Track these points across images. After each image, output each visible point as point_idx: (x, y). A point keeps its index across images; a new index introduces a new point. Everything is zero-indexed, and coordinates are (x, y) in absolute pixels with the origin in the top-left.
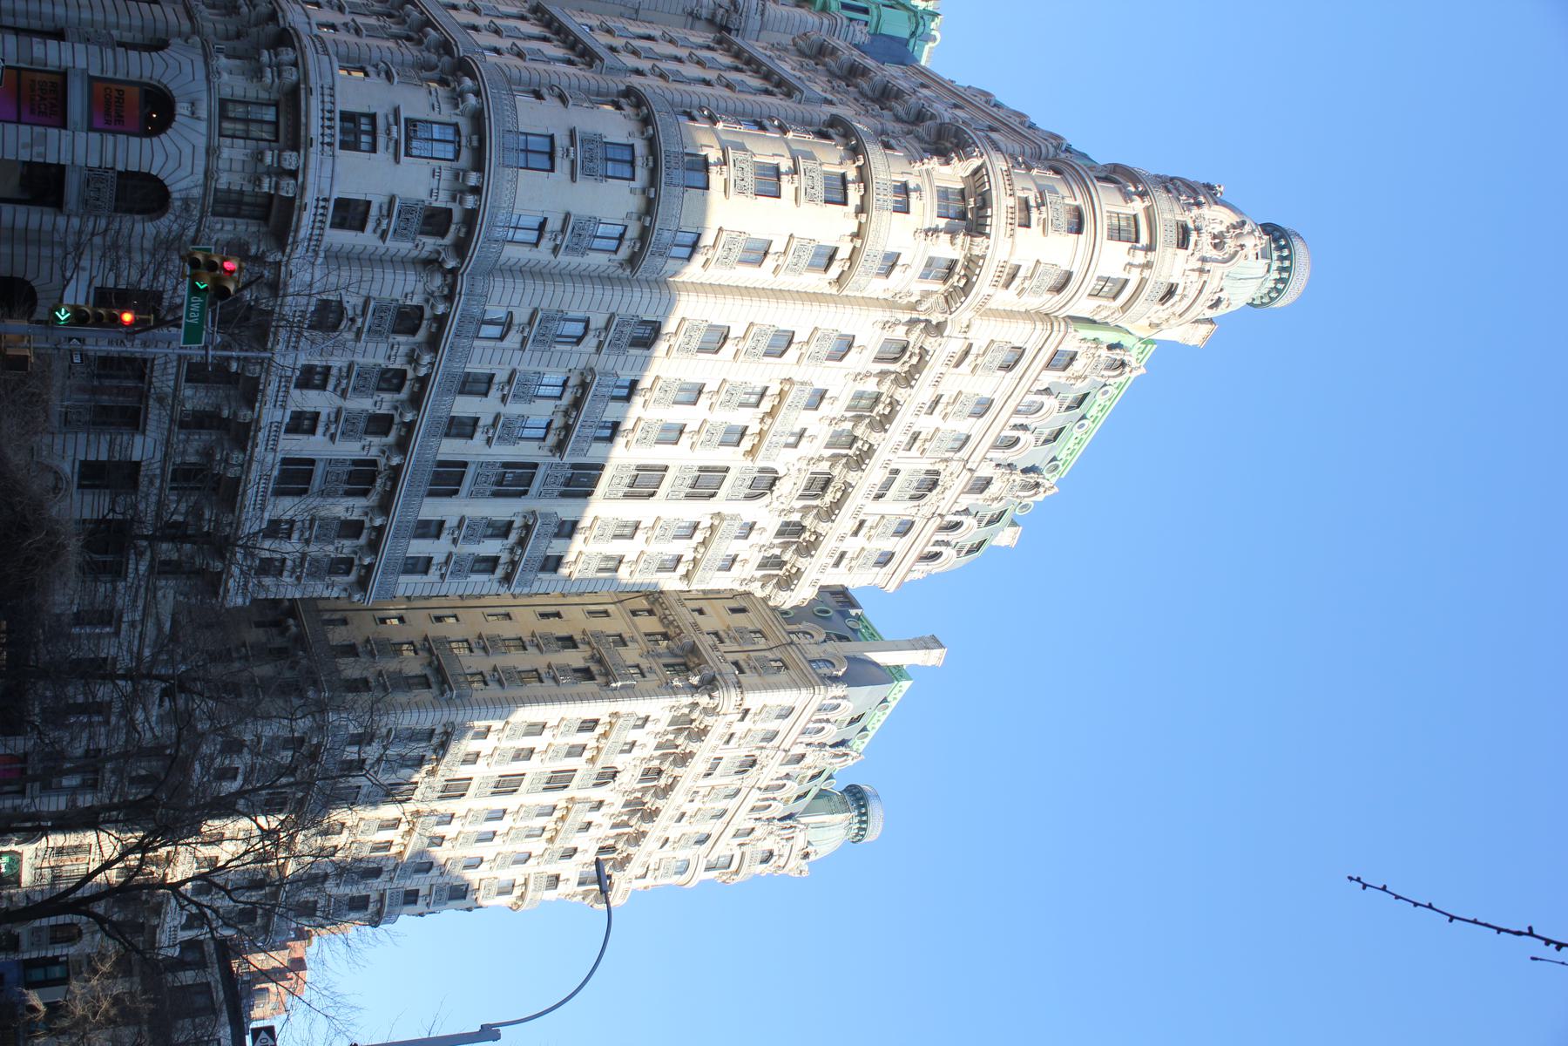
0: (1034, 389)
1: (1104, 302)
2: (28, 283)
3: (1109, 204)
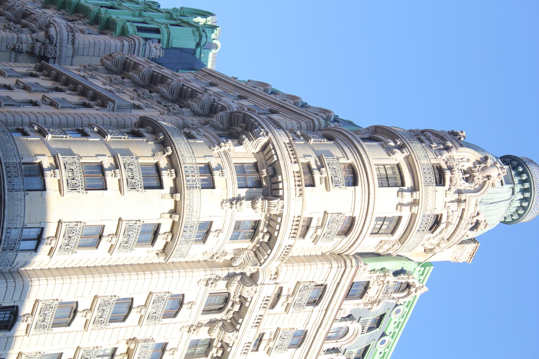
0: (339, 317)
1: (384, 238)
3: (376, 158)
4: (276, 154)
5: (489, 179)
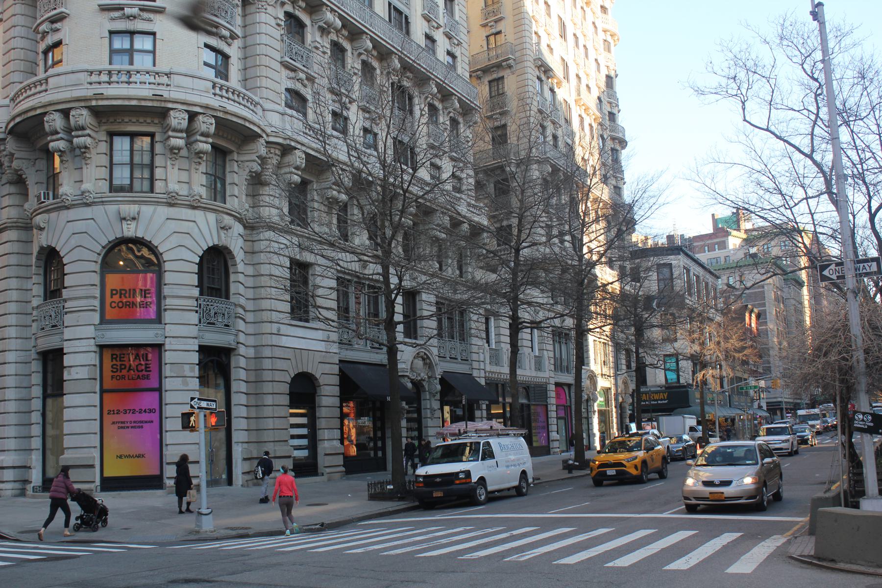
2: (292, 379)
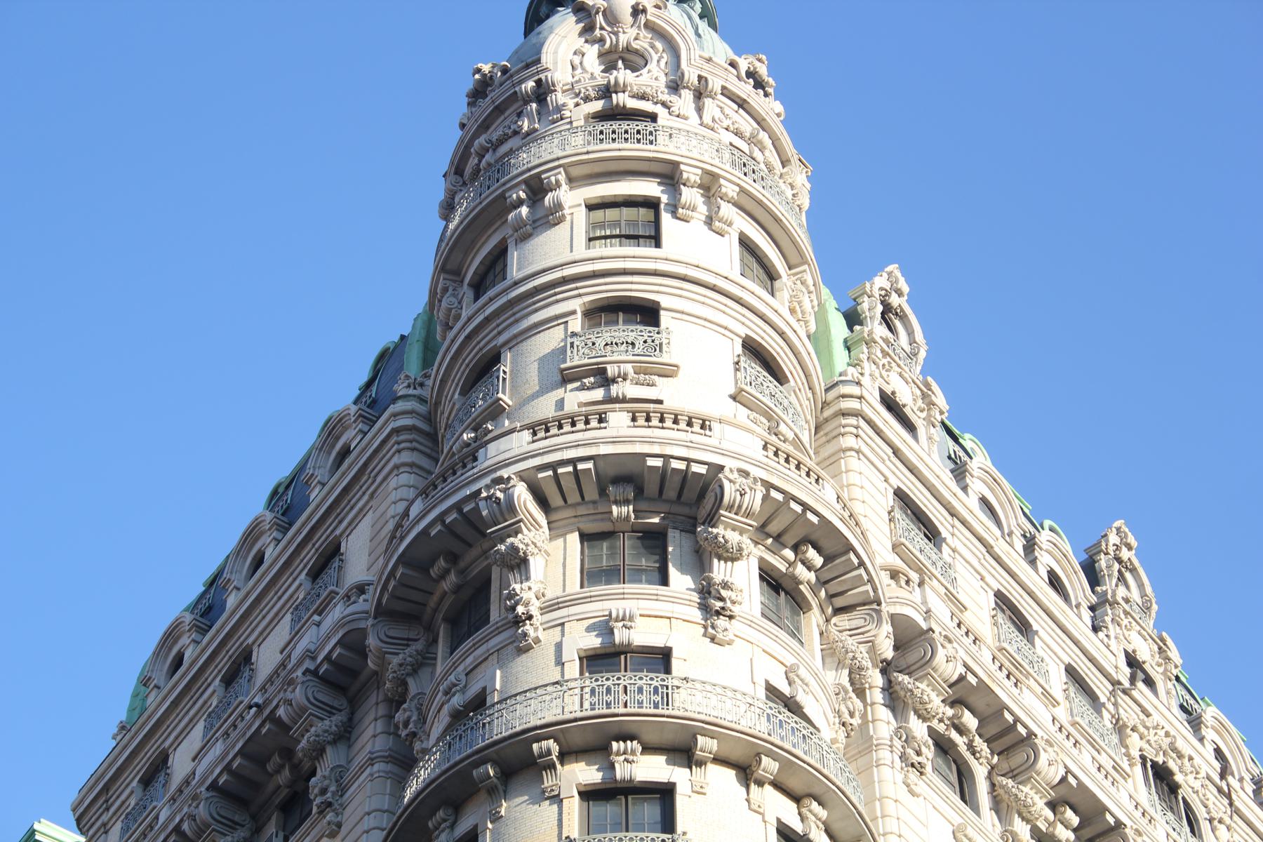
4: (573, 462)
5: (644, 11)
